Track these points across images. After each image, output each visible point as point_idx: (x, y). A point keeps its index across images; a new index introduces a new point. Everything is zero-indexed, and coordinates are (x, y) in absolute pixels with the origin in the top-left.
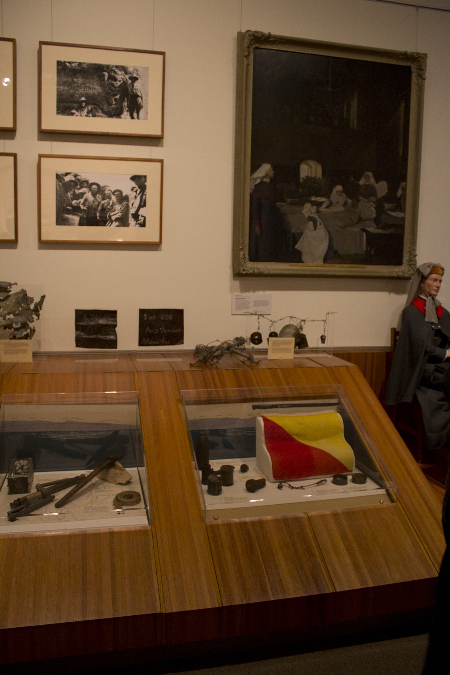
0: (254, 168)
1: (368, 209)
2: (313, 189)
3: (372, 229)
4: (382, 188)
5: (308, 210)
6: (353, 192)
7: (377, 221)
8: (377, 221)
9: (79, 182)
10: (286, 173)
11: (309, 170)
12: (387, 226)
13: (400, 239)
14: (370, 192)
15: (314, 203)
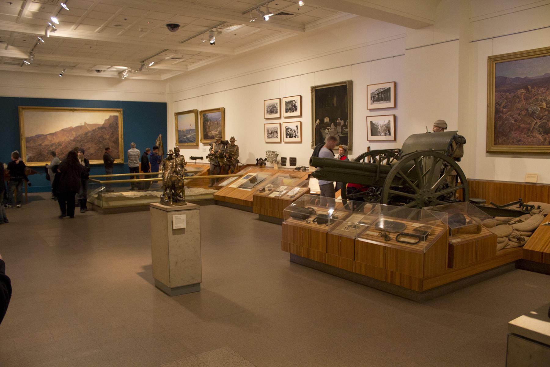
0: (316, 121)
1: (339, 129)
2: (328, 125)
3: (341, 135)
4: (342, 122)
5: (326, 131)
6: (336, 125)
7: (342, 132)
8: (342, 132)
9: (289, 128)
10: (322, 121)
11: (326, 120)
12: (344, 134)
13: (347, 137)
14: (340, 124)
15: (328, 129)
